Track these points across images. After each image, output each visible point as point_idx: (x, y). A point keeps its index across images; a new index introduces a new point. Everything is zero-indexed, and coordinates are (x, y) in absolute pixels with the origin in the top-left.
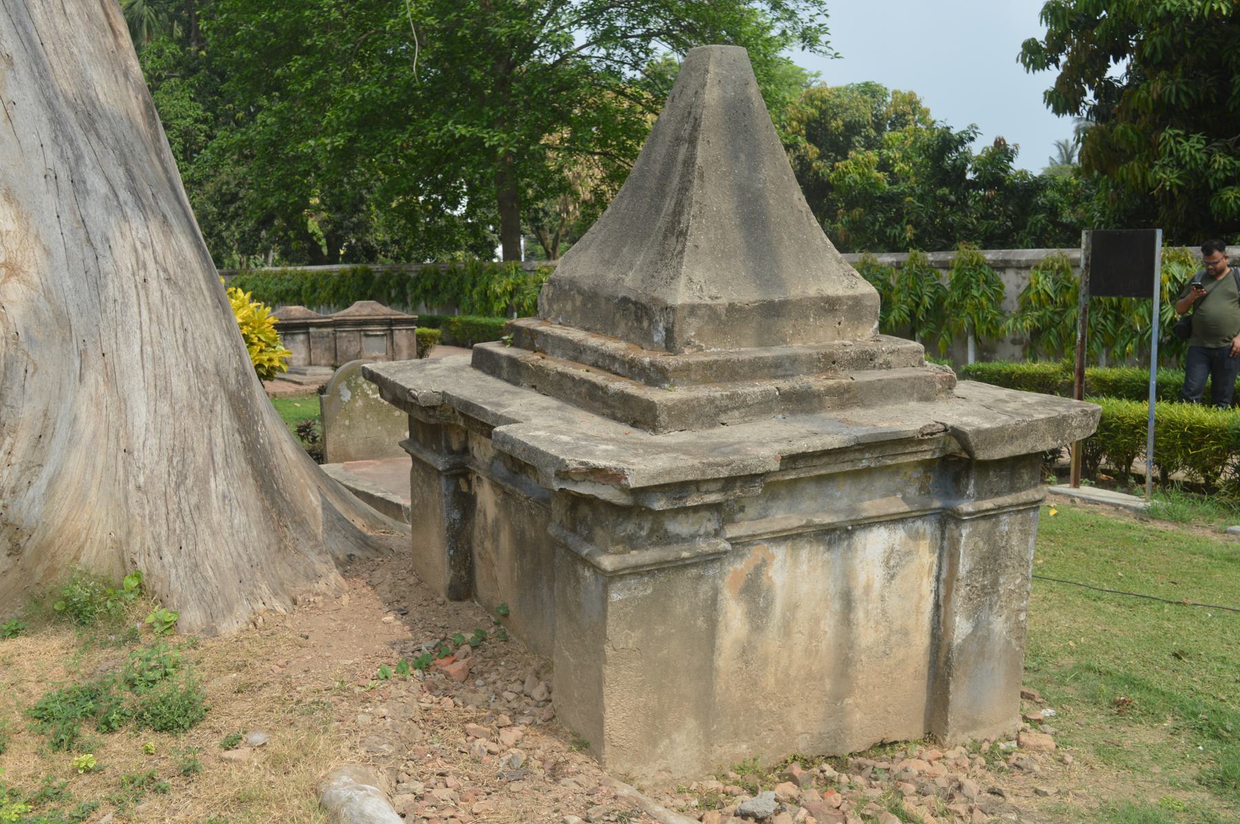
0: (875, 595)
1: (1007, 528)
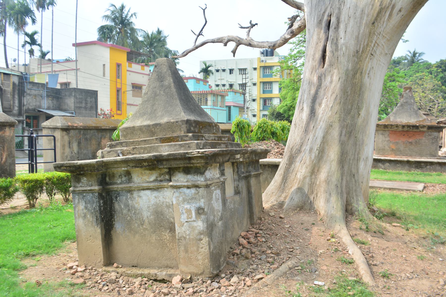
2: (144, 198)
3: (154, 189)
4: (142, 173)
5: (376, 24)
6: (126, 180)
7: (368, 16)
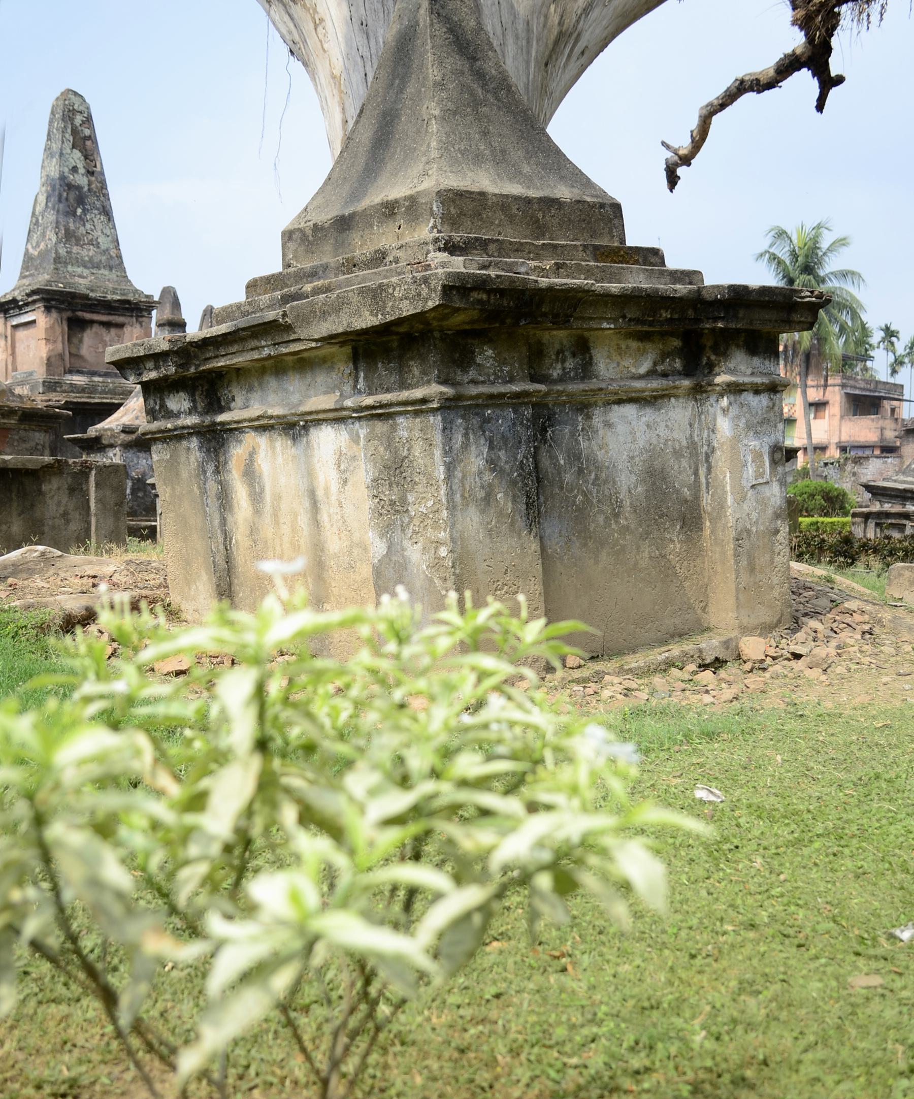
0: (333, 498)
1: (406, 434)
2: (621, 428)
3: (645, 399)
4: (619, 348)
5: (550, 66)
6: (575, 369)
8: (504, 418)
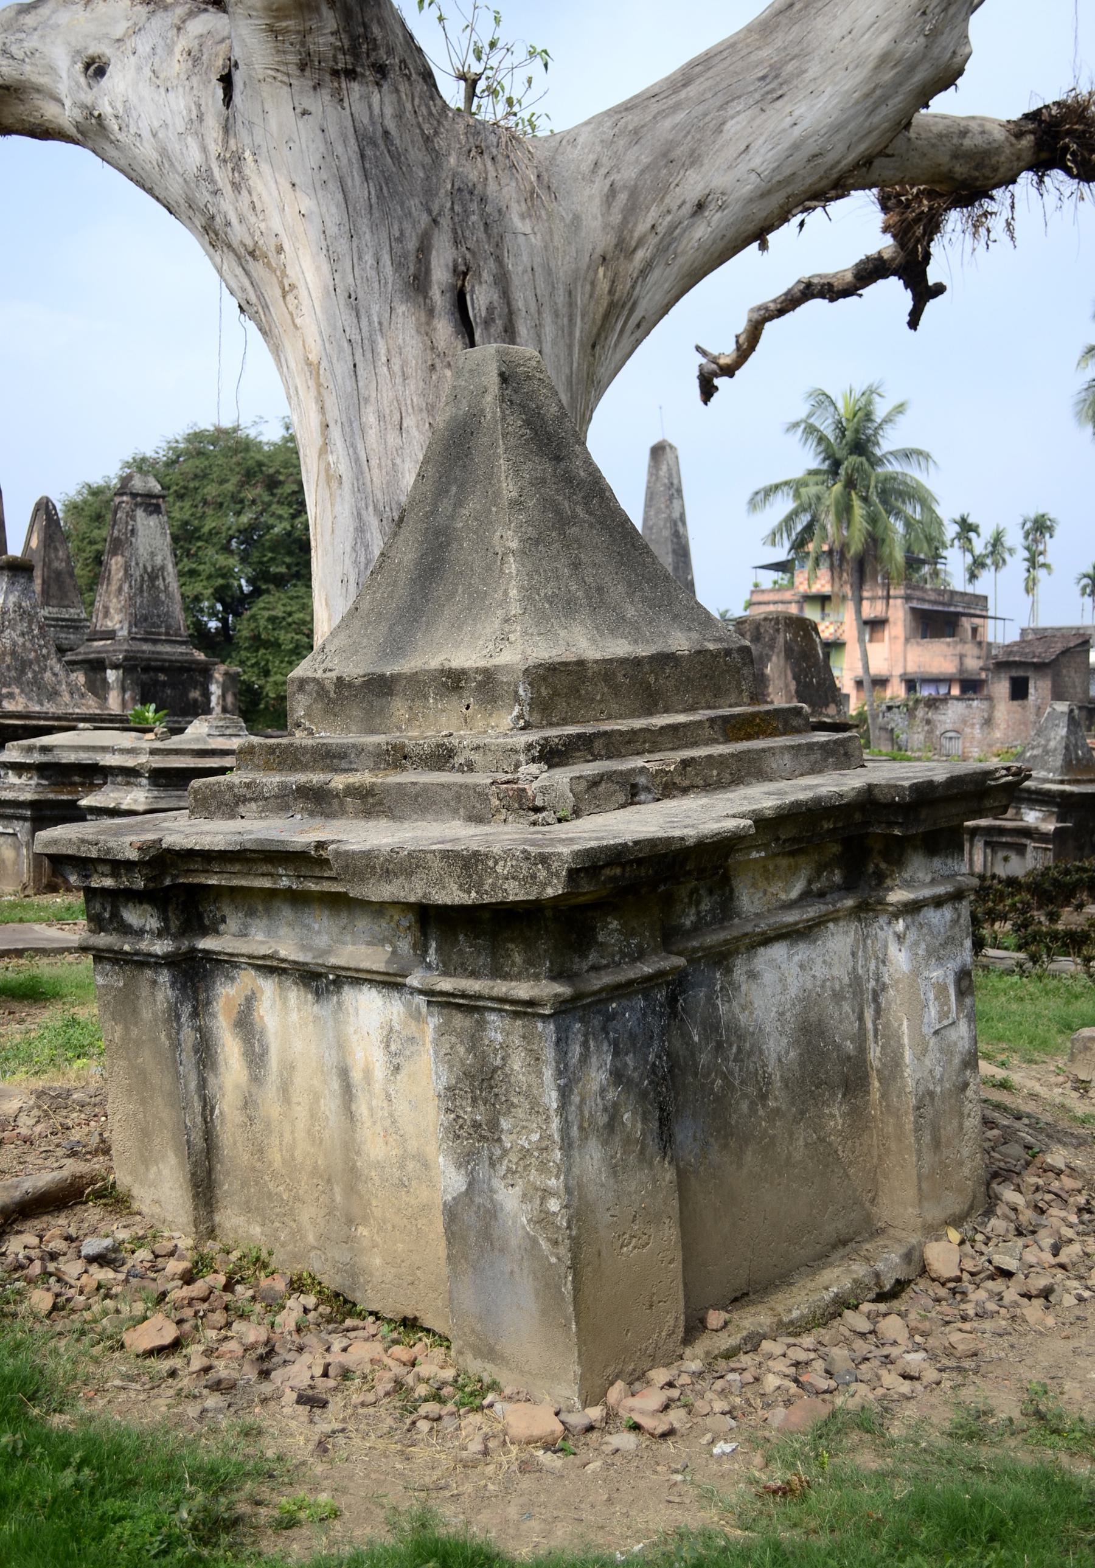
0: (378, 1086)
2: (769, 977)
3: (797, 932)
5: (598, 347)
6: (712, 910)
7: (583, 316)
8: (632, 1009)
